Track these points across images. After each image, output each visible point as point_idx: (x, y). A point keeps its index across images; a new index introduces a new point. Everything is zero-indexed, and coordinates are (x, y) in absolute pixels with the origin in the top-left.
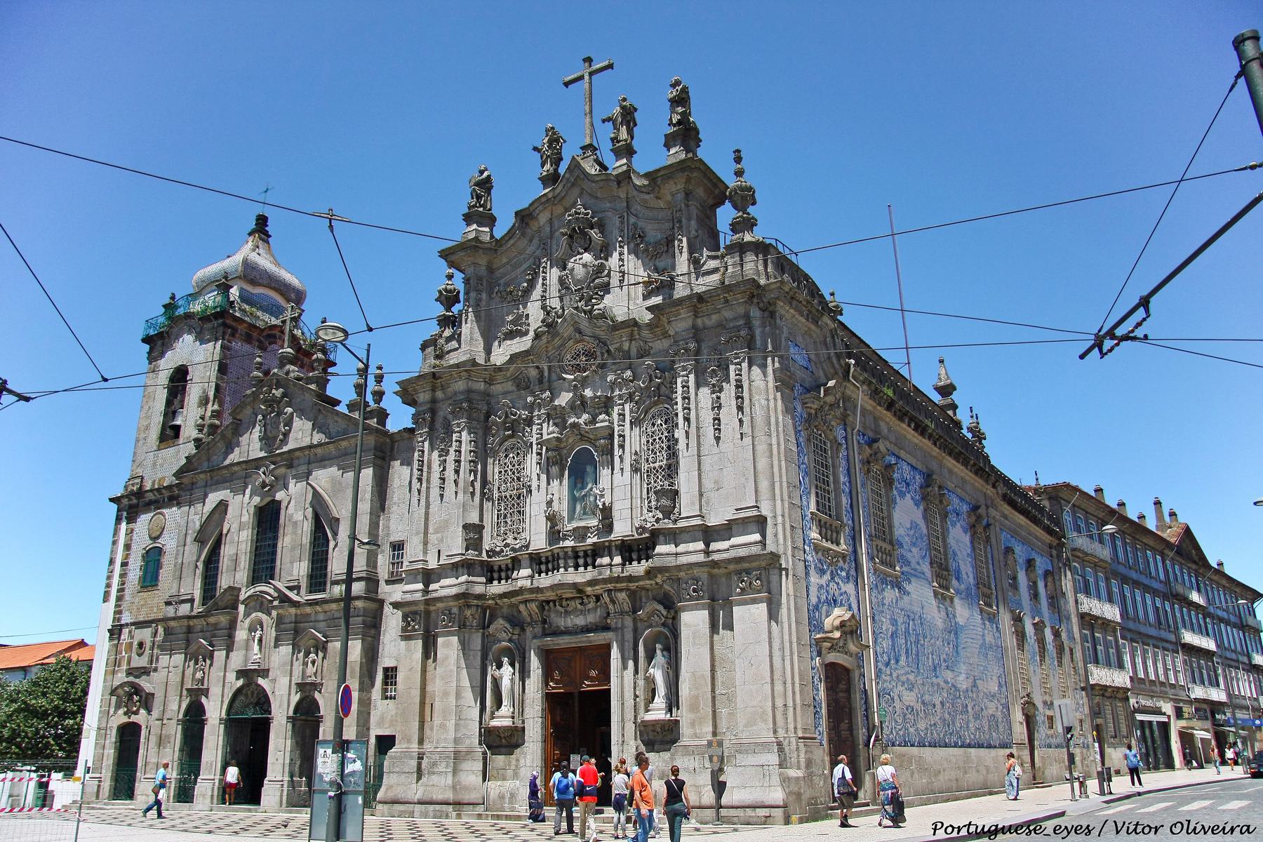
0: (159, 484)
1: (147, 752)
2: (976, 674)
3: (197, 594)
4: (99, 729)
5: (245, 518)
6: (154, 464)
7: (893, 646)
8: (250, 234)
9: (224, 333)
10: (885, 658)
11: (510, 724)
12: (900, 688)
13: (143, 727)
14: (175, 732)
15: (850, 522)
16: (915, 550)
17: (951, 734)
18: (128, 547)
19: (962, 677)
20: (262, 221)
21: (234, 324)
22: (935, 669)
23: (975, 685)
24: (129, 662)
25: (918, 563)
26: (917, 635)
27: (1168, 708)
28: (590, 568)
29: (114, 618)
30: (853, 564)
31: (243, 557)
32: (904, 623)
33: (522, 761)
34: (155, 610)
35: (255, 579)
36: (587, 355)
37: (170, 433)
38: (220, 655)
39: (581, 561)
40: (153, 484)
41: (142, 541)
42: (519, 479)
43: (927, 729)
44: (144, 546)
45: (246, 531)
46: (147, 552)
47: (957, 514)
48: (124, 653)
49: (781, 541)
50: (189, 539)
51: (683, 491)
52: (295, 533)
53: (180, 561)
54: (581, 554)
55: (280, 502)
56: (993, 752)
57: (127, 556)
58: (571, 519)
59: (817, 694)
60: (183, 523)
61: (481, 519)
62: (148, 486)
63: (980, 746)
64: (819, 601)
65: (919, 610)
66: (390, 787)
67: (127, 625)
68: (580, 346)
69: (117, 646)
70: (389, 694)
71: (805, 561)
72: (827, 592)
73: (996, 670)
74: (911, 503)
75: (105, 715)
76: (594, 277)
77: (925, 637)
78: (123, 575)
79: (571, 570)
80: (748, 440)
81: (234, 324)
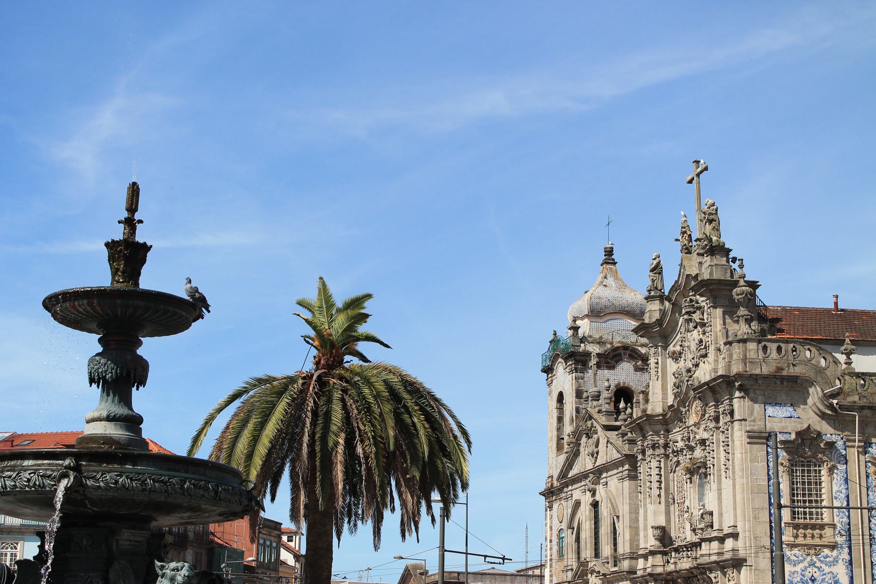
5: (587, 514)
8: (602, 265)
9: (576, 369)
15: (845, 520)
18: (551, 528)
20: (609, 252)
21: (582, 358)
30: (846, 550)
41: (556, 525)
52: (605, 524)
55: (598, 502)
57: (552, 534)
61: (668, 521)
72: (803, 575)
76: (699, 348)
78: (551, 549)
79: (685, 559)
81: (582, 358)
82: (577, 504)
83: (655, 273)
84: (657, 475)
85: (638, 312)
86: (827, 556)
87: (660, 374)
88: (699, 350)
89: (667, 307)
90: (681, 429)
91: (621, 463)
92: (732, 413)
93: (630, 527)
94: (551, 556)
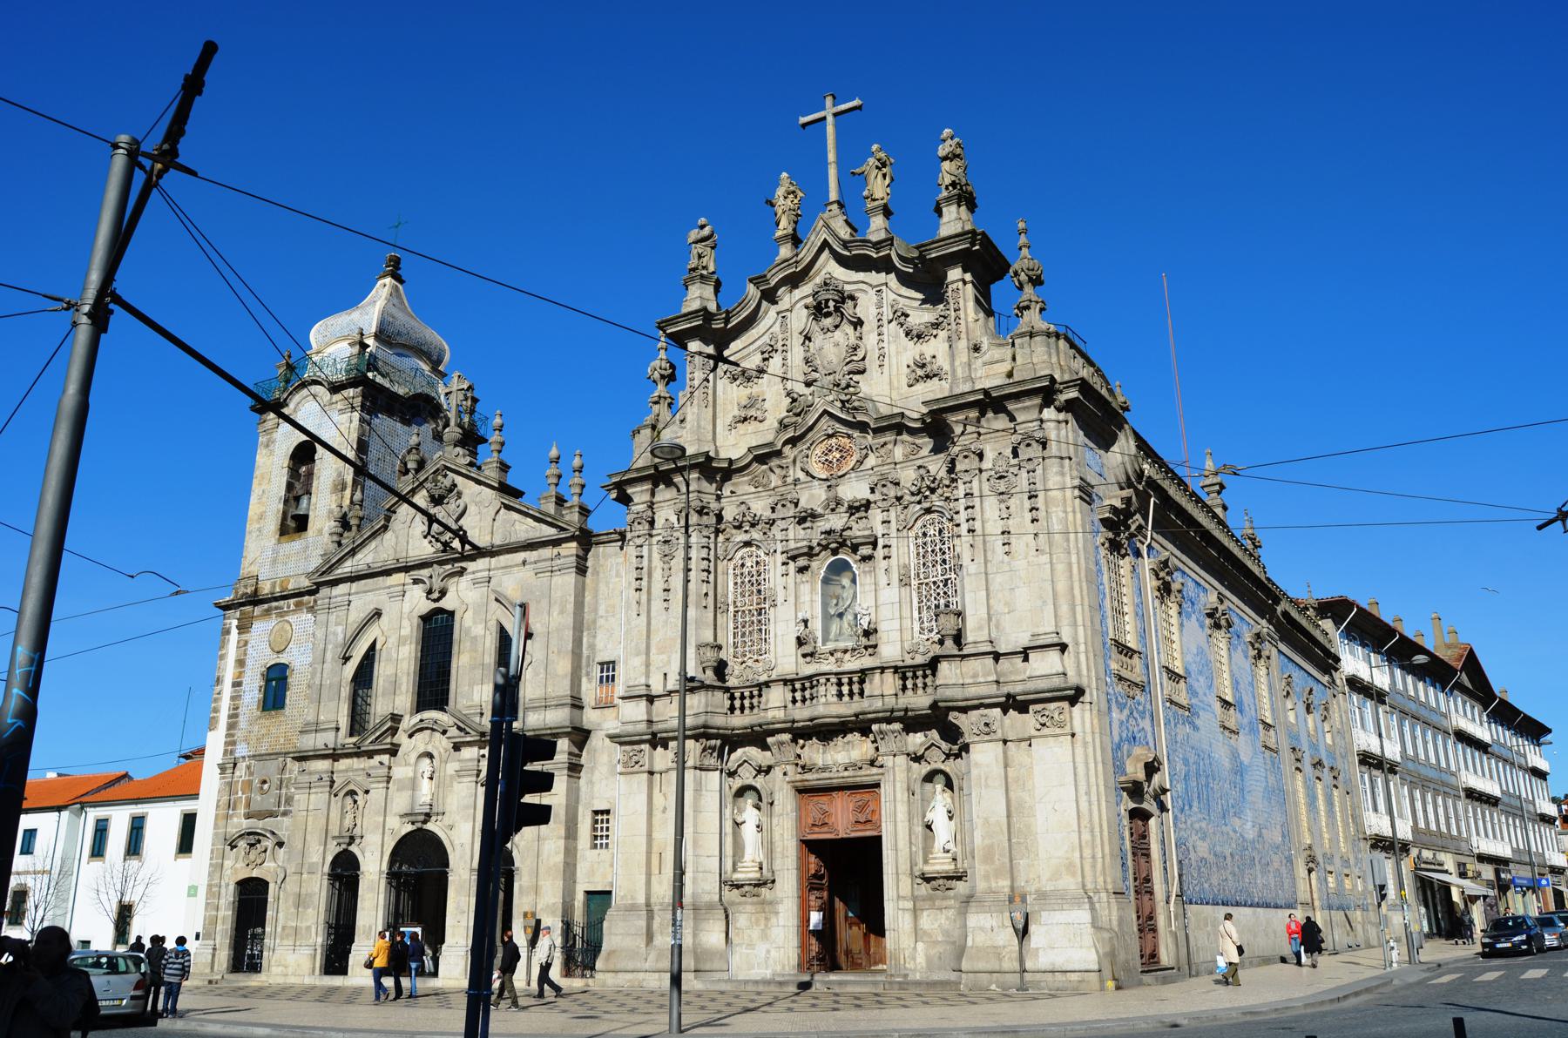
0: (281, 586)
1: (279, 913)
2: (1261, 822)
3: (344, 722)
4: (210, 886)
6: (274, 561)
7: (1186, 789)
9: (363, 406)
10: (1180, 802)
11: (757, 875)
12: (1194, 838)
13: (271, 886)
14: (318, 888)
16: (1202, 679)
17: (1241, 891)
18: (241, 663)
19: (1249, 824)
22: (1224, 817)
23: (1260, 835)
24: (248, 805)
25: (1205, 695)
26: (1207, 777)
27: (1449, 862)
28: (856, 698)
29: (225, 752)
31: (404, 679)
32: (1194, 763)
33: (774, 920)
34: (282, 740)
35: (422, 704)
36: (841, 451)
37: (292, 524)
38: (377, 792)
39: (845, 689)
40: (274, 585)
41: (261, 656)
42: (759, 592)
43: (1219, 884)
44: (263, 662)
45: (407, 647)
46: (268, 669)
47: (1238, 636)
48: (240, 793)
49: (1085, 672)
50: (329, 655)
51: (969, 613)
53: (318, 682)
54: (845, 680)
55: (452, 614)
56: (1279, 911)
57: (241, 673)
58: (825, 641)
59: (1123, 844)
60: (320, 634)
62: (266, 589)
63: (1267, 906)
64: (1121, 738)
65: (1208, 748)
66: (611, 953)
67: (244, 757)
68: (833, 441)
69: (230, 784)
70: (598, 842)
71: (1108, 694)
72: (1127, 728)
73: (1278, 818)
74: (1196, 625)
75: (217, 868)
76: (848, 360)
77: (1214, 780)
79: (835, 699)
80: (1045, 558)
82: (378, 614)
83: (705, 246)
84: (703, 559)
85: (435, 358)
86: (1139, 704)
87: (710, 398)
88: (848, 363)
89: (751, 293)
90: (760, 489)
91: (556, 543)
92: (1044, 444)
93: (573, 652)
94: (234, 709)
